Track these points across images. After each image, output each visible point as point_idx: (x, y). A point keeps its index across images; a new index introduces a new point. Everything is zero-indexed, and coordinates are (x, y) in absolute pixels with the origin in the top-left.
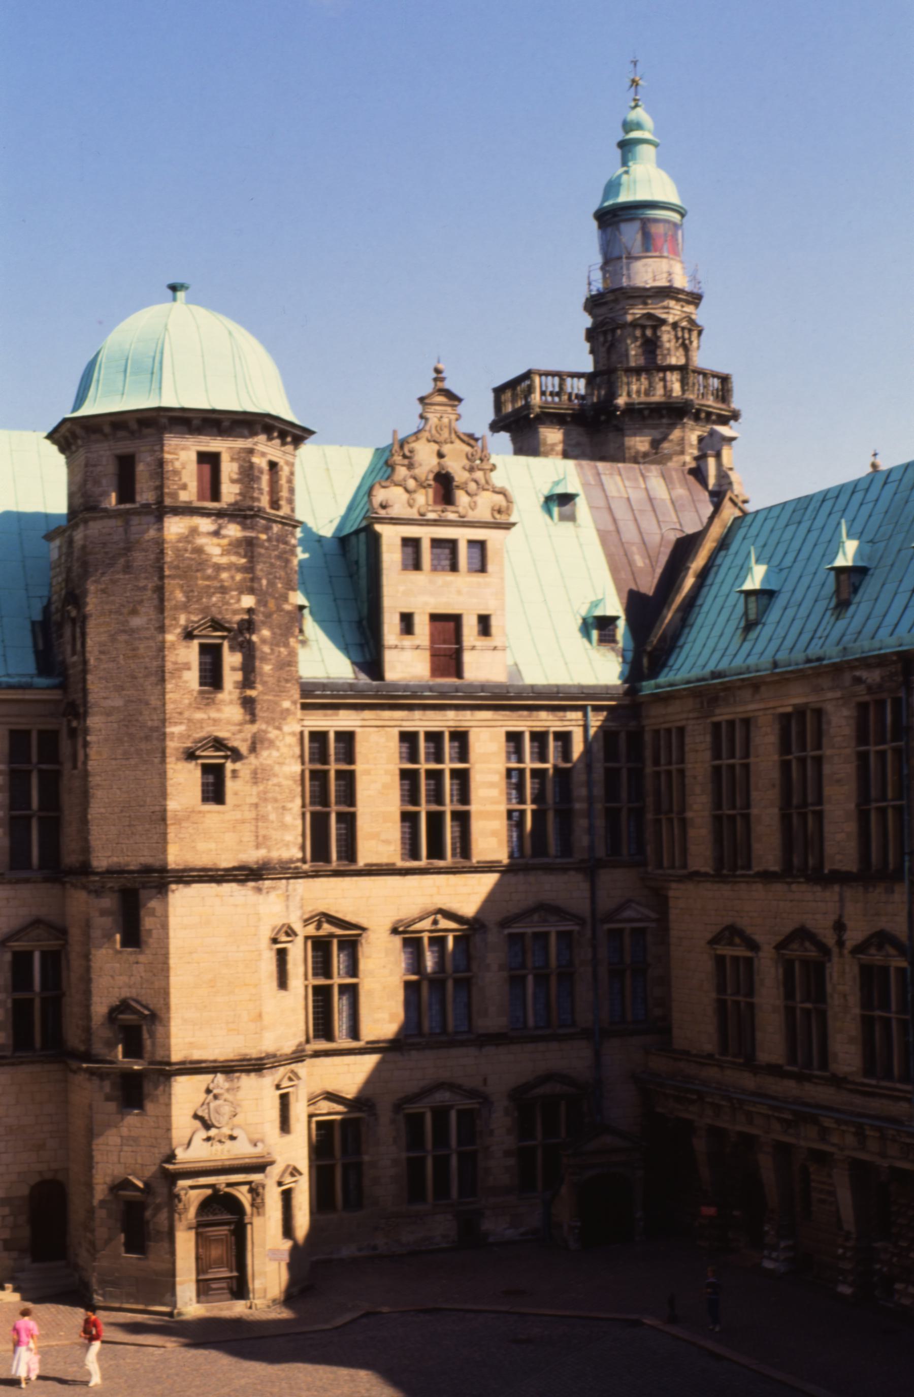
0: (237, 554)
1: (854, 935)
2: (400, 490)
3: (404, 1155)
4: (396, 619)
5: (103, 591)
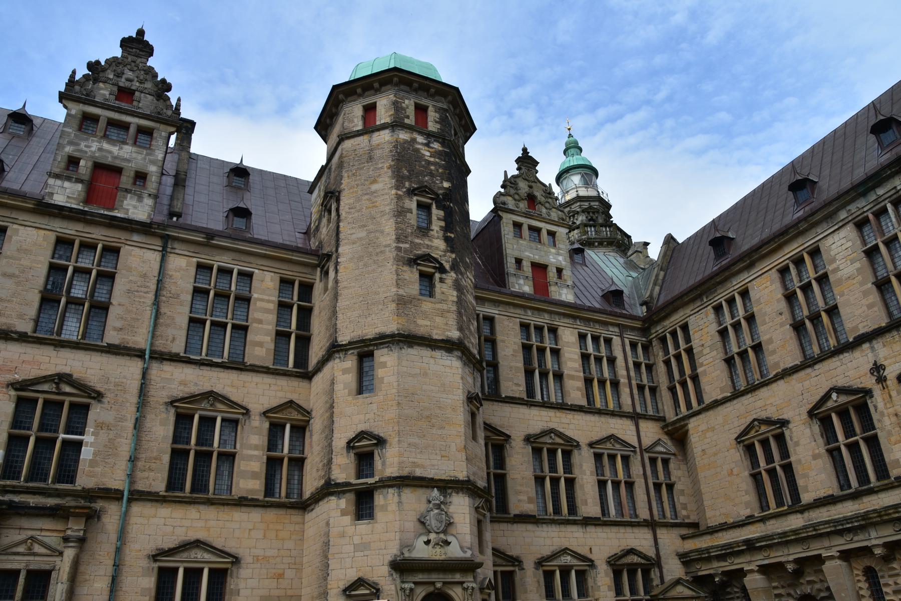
0: (438, 158)
2: (510, 198)
4: (513, 261)
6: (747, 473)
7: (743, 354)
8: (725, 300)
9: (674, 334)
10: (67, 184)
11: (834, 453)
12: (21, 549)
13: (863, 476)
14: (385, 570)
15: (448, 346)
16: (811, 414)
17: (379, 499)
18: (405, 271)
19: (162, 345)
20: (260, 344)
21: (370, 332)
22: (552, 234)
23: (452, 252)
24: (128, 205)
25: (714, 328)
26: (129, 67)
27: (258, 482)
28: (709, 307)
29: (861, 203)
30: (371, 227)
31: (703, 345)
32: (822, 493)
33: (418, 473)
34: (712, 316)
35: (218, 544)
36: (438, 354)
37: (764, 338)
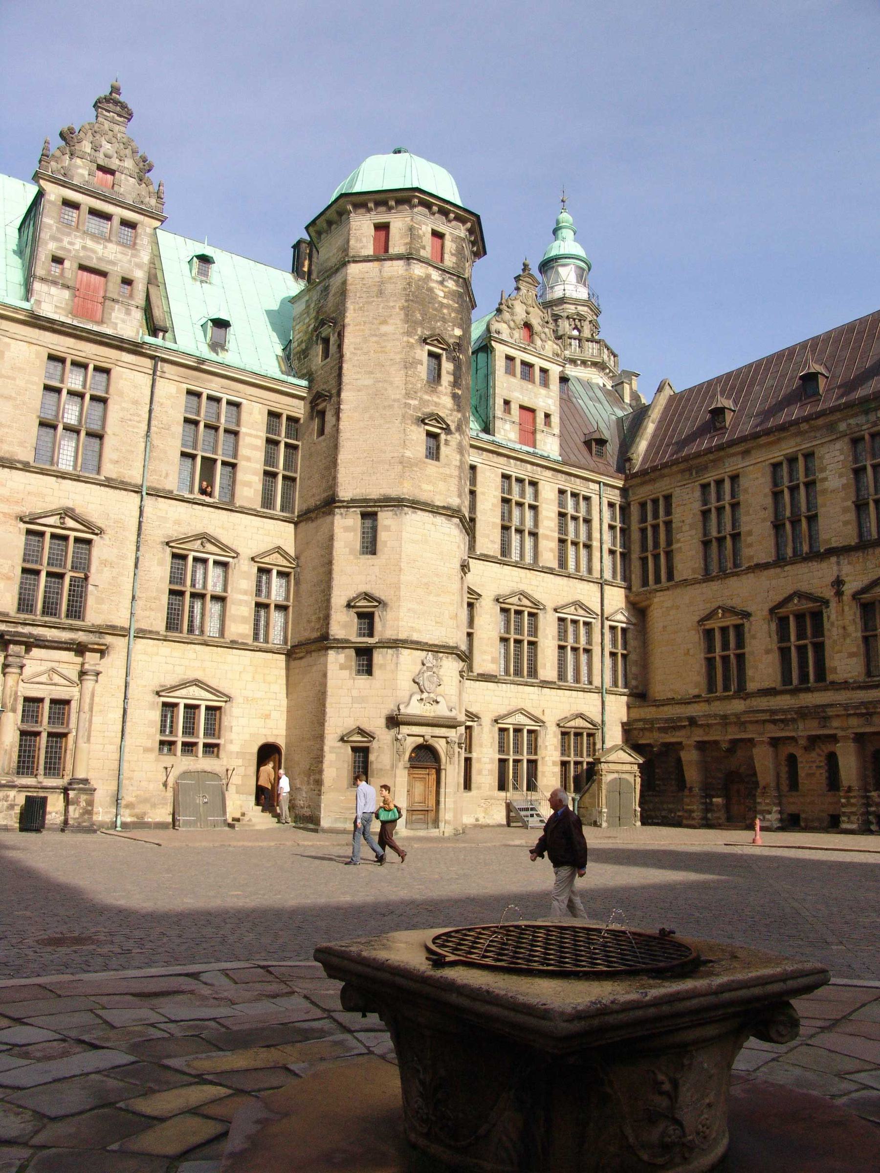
0: (453, 300)
1: (850, 588)
2: (505, 326)
3: (498, 756)
5: (361, 309)
6: (702, 655)
7: (721, 540)
8: (715, 481)
9: (655, 502)
10: (54, 290)
11: (784, 653)
12: (44, 678)
13: (804, 677)
14: (382, 722)
15: (450, 512)
16: (772, 611)
17: (378, 657)
18: (413, 431)
19: (153, 481)
20: (248, 484)
21: (374, 493)
22: (544, 371)
23: (459, 411)
24: (117, 318)
25: (697, 506)
26: (107, 137)
27: (247, 627)
28: (697, 484)
29: (861, 419)
30: (379, 375)
31: (683, 521)
32: (766, 685)
33: (415, 637)
34: (698, 494)
35: (213, 683)
36: (440, 520)
37: (744, 529)
